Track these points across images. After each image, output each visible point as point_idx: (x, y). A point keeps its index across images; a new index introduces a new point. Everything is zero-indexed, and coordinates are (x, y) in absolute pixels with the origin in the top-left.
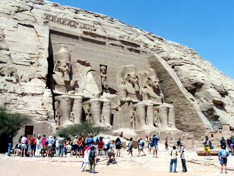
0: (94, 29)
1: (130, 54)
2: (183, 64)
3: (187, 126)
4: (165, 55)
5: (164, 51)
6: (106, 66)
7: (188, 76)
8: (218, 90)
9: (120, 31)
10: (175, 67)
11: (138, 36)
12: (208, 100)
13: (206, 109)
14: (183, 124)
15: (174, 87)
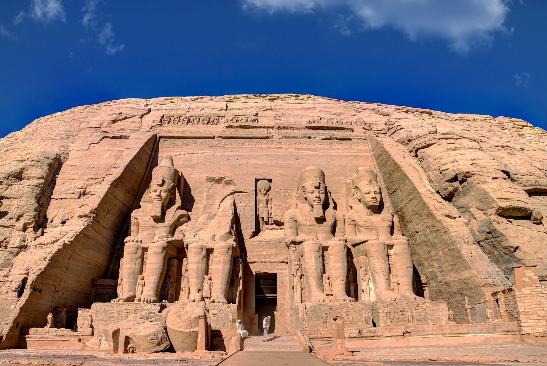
0: (254, 118)
1: (330, 149)
2: (434, 141)
3: (446, 283)
4: (403, 134)
5: (401, 129)
6: (270, 181)
7: (439, 165)
8: (524, 183)
9: (316, 113)
10: (418, 153)
11: (358, 114)
12: (485, 210)
13: (483, 234)
14: (440, 279)
15: (414, 197)
